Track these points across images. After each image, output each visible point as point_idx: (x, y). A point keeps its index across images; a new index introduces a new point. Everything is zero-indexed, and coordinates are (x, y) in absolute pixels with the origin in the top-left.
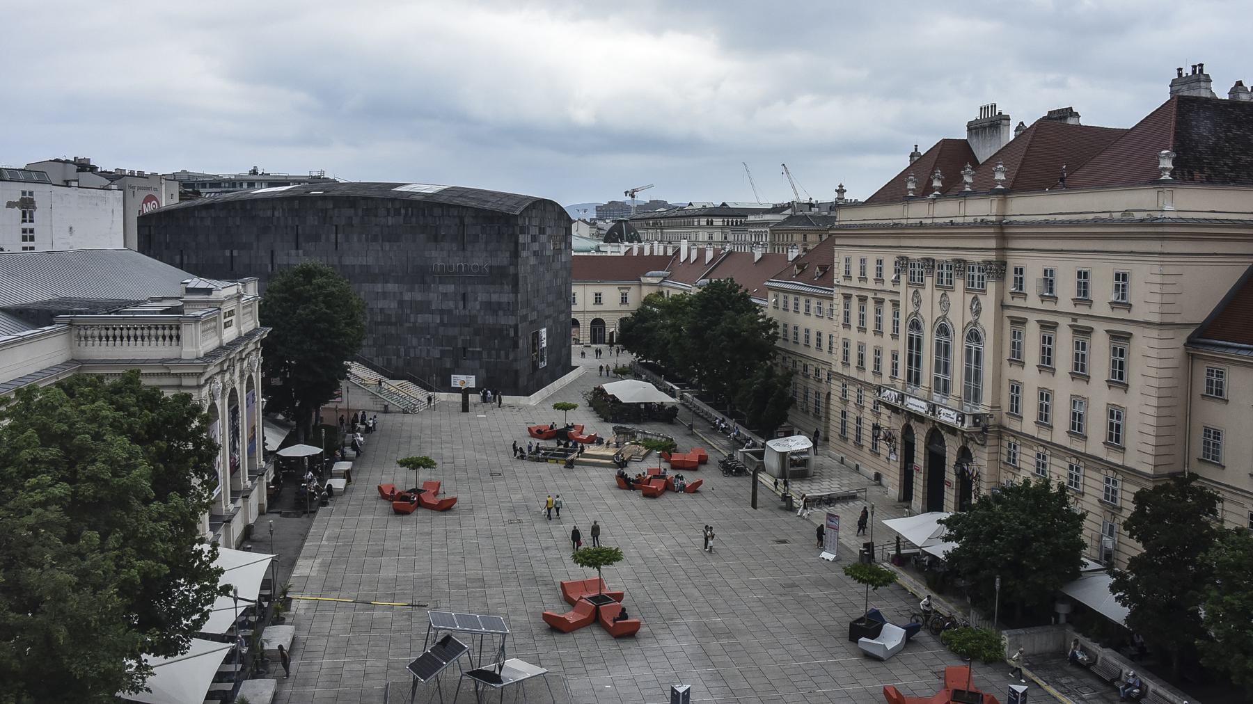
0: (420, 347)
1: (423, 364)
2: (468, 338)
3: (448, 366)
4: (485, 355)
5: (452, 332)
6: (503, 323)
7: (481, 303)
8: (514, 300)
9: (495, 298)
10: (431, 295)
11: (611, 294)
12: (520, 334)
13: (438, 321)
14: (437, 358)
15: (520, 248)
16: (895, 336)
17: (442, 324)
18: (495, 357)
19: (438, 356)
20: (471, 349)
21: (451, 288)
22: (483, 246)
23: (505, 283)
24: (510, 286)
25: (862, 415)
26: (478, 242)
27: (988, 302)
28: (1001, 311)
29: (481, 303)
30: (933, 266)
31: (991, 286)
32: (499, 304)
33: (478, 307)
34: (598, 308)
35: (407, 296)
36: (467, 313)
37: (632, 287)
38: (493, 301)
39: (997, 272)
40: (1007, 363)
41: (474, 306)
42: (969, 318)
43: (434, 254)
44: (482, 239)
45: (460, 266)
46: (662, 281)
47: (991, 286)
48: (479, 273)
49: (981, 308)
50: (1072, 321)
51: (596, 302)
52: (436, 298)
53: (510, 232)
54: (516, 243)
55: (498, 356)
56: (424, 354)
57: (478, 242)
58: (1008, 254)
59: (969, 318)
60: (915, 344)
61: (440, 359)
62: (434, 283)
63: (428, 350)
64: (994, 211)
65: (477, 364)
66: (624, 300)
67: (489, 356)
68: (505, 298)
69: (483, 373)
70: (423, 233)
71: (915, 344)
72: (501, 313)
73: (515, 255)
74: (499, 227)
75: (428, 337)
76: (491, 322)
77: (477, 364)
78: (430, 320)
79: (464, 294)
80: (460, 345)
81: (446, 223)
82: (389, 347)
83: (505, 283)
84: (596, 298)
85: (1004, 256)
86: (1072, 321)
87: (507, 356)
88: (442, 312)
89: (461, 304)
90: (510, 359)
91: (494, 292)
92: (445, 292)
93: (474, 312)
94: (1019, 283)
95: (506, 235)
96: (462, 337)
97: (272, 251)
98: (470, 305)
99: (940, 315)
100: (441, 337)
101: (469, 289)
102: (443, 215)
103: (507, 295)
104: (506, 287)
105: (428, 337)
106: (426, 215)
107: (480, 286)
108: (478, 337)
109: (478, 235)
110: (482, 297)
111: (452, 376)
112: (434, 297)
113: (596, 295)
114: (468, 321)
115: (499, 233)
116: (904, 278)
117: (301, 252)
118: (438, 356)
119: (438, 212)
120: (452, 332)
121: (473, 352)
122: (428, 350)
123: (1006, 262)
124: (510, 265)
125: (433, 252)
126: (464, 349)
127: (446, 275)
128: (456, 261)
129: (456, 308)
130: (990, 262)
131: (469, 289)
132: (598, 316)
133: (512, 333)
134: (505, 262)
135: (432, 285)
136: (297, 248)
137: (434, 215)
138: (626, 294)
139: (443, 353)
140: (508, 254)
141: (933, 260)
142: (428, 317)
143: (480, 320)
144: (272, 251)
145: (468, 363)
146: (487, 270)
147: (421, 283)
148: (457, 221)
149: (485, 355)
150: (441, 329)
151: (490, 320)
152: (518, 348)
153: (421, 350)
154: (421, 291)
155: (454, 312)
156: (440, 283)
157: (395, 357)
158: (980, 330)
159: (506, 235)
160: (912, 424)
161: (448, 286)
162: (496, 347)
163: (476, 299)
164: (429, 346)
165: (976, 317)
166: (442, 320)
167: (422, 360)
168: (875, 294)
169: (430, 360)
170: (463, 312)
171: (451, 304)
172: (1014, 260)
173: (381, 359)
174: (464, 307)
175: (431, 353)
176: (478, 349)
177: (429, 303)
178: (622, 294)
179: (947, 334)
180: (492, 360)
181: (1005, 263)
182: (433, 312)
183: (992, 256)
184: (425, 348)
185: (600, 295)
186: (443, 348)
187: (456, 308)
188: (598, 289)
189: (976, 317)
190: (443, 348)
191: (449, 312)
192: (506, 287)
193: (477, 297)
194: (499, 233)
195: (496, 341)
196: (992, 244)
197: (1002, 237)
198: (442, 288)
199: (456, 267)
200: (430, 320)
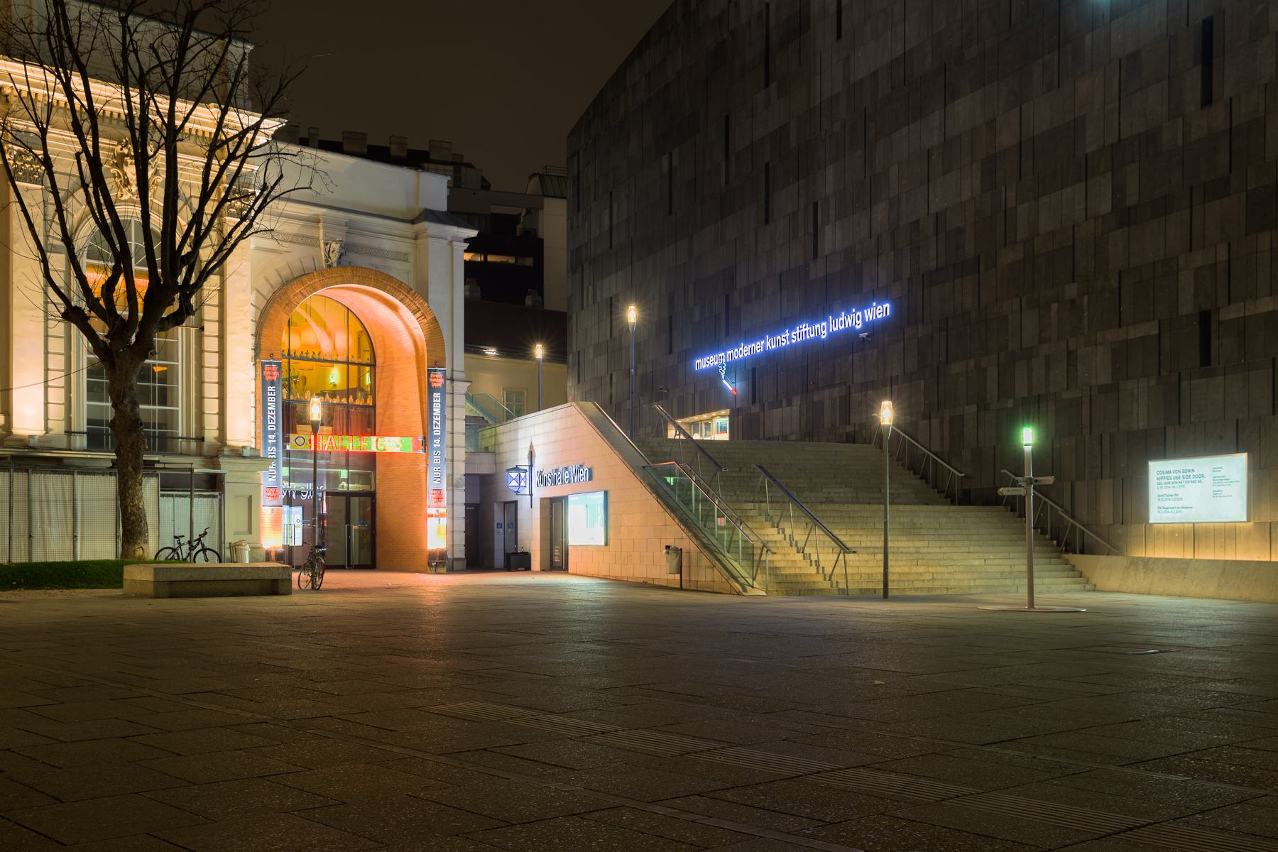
2: (1222, 255)
13: (1105, 207)
14: (1104, 389)
17: (1124, 216)
19: (1104, 379)
20: (1230, 314)
35: (1007, 138)
80: (1187, 306)
82: (957, 368)
97: (727, 118)
100: (1115, 284)
105: (1072, 291)
117: (773, 86)
118: (1104, 379)
126: (1205, 319)
136: (767, 85)
144: (727, 118)
157: (973, 408)
173: (935, 422)
174: (1207, 101)
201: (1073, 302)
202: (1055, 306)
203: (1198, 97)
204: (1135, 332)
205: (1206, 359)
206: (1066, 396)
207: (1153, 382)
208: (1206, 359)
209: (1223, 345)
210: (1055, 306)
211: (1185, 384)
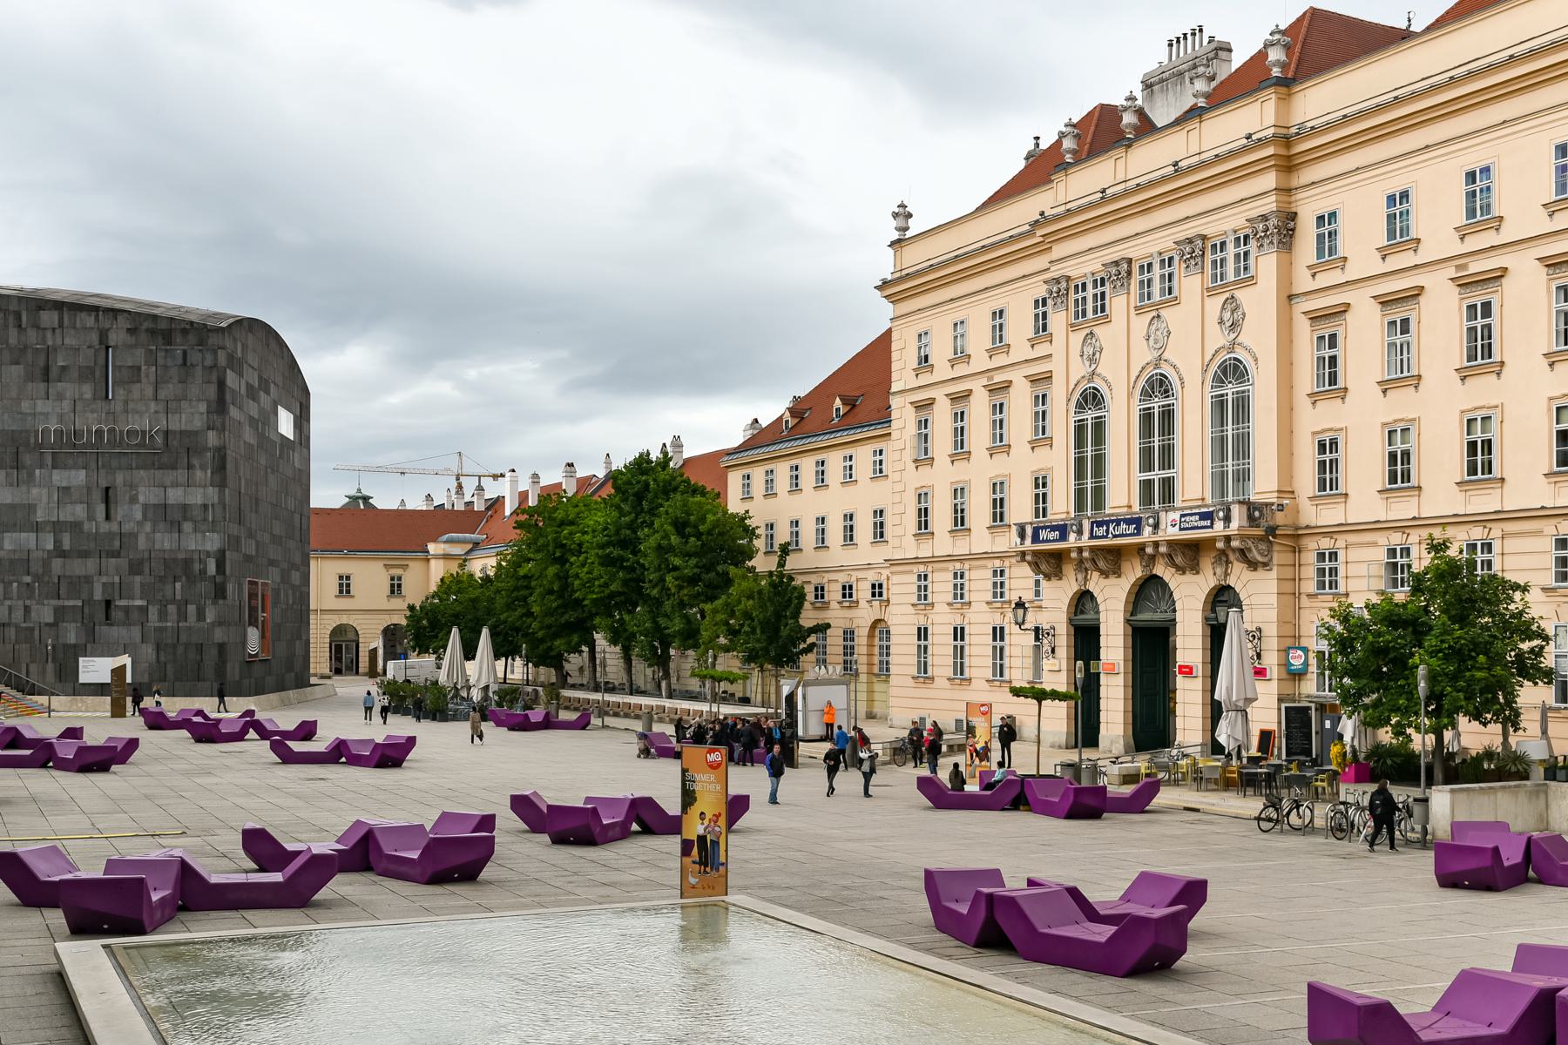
0: (8, 603)
1: (13, 637)
2: (117, 579)
3: (72, 638)
4: (153, 613)
5: (78, 567)
6: (193, 547)
7: (146, 507)
8: (216, 500)
9: (175, 496)
10: (35, 491)
11: (370, 576)
12: (228, 573)
13: (50, 546)
14: (47, 624)
15: (228, 397)
16: (1041, 437)
17: (60, 552)
18: (175, 617)
19: (50, 619)
21: (78, 477)
22: (149, 391)
23: (197, 466)
24: (209, 472)
25: (966, 621)
26: (139, 381)
27: (1260, 301)
28: (1288, 306)
29: (146, 507)
30: (1129, 273)
31: (1266, 264)
32: (185, 508)
33: (139, 516)
34: (344, 603)
36: (114, 527)
37: (411, 564)
38: (171, 501)
39: (1279, 233)
40: (1308, 401)
41: (130, 515)
42: (1217, 338)
43: (41, 406)
44: (147, 376)
45: (99, 432)
46: (471, 550)
47: (1266, 264)
48: (142, 445)
49: (1244, 314)
50: (1456, 272)
51: (341, 592)
52: (45, 499)
53: (208, 362)
54: (221, 384)
55: (182, 616)
56: (18, 615)
57: (139, 381)
58: (1299, 196)
59: (1217, 338)
60: (1089, 437)
61: (55, 625)
62: (41, 467)
63: (27, 609)
64: (1270, 119)
65: (136, 632)
66: (396, 589)
67: (163, 615)
68: (196, 497)
69: (148, 651)
70: (17, 363)
71: (1089, 437)
72: (187, 527)
73: (220, 405)
74: (185, 353)
75: (28, 579)
76: (167, 546)
77: (136, 632)
78: (33, 545)
79: (107, 489)
80: (98, 595)
81: (67, 341)
83: (197, 466)
84: (341, 585)
85: (1290, 203)
86: (1456, 272)
87: (201, 616)
88: (57, 527)
89: (100, 510)
90: (208, 621)
91: (175, 485)
92: (64, 484)
93: (127, 528)
94: (1327, 242)
95: (199, 368)
96: (104, 579)
98: (120, 512)
99: (1148, 359)
100: (56, 581)
101: (120, 478)
102: (61, 325)
103: (201, 490)
104: (199, 474)
105: (28, 579)
106: (23, 326)
107: (142, 472)
108: (138, 579)
109: (139, 368)
110: (147, 495)
111: (81, 659)
112: (38, 494)
113: (341, 578)
114: (117, 544)
115: (185, 364)
116: (1058, 320)
118: (50, 619)
119: (49, 318)
120: (78, 567)
121: (127, 610)
122: (27, 609)
123: (1296, 213)
124: (209, 428)
125: (39, 402)
126: (108, 603)
127: (68, 449)
128: (91, 421)
129: (91, 518)
130: (1264, 218)
131: (120, 478)
132: (344, 620)
133: (212, 568)
134: (198, 423)
135: (37, 471)
137: (43, 326)
138: (400, 578)
139: (60, 613)
140: (203, 407)
141: (1130, 261)
142: (28, 539)
143: (142, 543)
145: (115, 633)
146: (159, 440)
147: (12, 468)
148: (94, 338)
149: (153, 613)
150: (57, 564)
151: (165, 541)
152: (225, 598)
153: (10, 608)
154: (11, 485)
155: (86, 527)
156: (53, 468)
158: (1240, 354)
159: (199, 368)
160: (1091, 587)
161: (73, 472)
162: (178, 597)
163: (134, 500)
164: (28, 599)
165: (1233, 336)
166: (57, 542)
167: (13, 630)
168: (990, 378)
169: (32, 629)
170: (105, 527)
171: (80, 511)
172: (1308, 209)
174: (108, 517)
175: (33, 614)
176: (139, 603)
177: (31, 508)
178: (392, 579)
179: (1166, 393)
180: (169, 624)
181: (1293, 216)
182: (37, 528)
183: (1269, 205)
184: (21, 602)
185: (348, 578)
186: (60, 603)
187: (91, 518)
188: (344, 567)
189: (1233, 336)
190: (60, 603)
191: (75, 526)
192: (199, 474)
193: (137, 495)
194: (185, 364)
195: (178, 585)
196: (1269, 180)
197: (1288, 165)
198: (59, 478)
199: (89, 431)
200: (33, 545)
201: (28, 584)
202: (15, 585)
203: (104, 515)
204: (71, 603)
205: (108, 618)
206: (24, 625)
207: (79, 625)
208: (108, 618)
209: (117, 615)
210: (15, 585)
211: (97, 628)
